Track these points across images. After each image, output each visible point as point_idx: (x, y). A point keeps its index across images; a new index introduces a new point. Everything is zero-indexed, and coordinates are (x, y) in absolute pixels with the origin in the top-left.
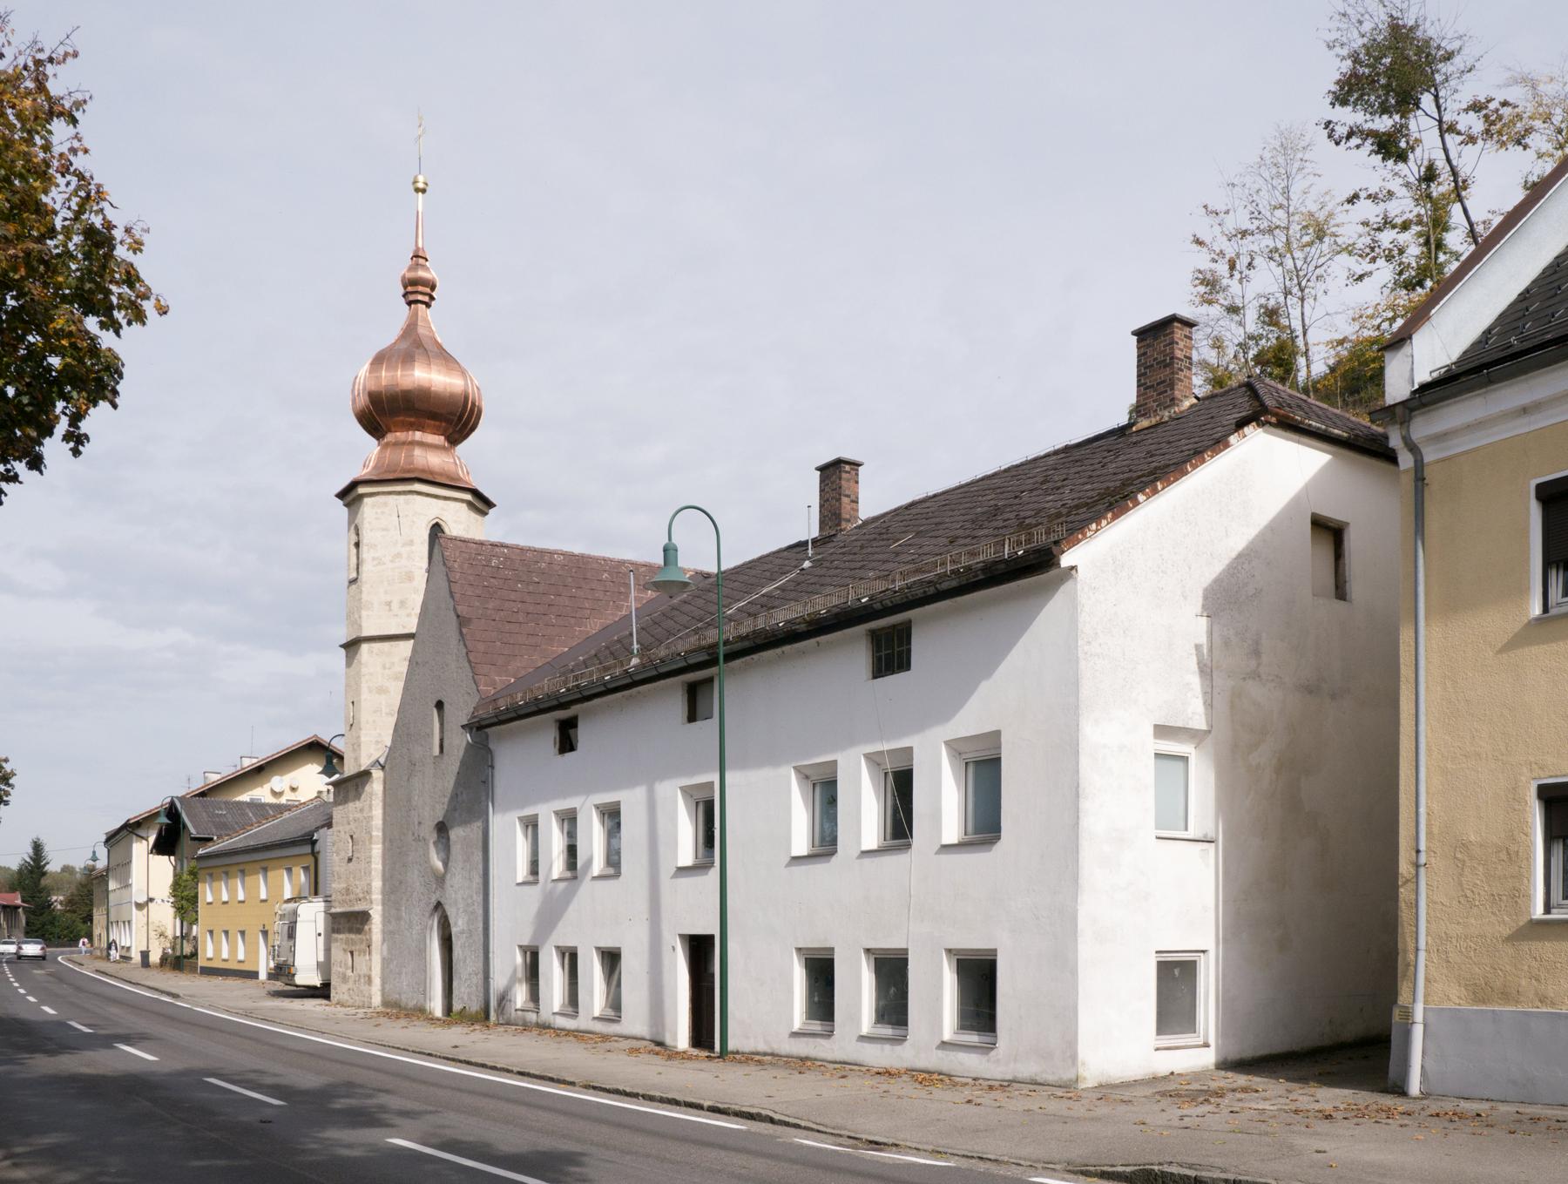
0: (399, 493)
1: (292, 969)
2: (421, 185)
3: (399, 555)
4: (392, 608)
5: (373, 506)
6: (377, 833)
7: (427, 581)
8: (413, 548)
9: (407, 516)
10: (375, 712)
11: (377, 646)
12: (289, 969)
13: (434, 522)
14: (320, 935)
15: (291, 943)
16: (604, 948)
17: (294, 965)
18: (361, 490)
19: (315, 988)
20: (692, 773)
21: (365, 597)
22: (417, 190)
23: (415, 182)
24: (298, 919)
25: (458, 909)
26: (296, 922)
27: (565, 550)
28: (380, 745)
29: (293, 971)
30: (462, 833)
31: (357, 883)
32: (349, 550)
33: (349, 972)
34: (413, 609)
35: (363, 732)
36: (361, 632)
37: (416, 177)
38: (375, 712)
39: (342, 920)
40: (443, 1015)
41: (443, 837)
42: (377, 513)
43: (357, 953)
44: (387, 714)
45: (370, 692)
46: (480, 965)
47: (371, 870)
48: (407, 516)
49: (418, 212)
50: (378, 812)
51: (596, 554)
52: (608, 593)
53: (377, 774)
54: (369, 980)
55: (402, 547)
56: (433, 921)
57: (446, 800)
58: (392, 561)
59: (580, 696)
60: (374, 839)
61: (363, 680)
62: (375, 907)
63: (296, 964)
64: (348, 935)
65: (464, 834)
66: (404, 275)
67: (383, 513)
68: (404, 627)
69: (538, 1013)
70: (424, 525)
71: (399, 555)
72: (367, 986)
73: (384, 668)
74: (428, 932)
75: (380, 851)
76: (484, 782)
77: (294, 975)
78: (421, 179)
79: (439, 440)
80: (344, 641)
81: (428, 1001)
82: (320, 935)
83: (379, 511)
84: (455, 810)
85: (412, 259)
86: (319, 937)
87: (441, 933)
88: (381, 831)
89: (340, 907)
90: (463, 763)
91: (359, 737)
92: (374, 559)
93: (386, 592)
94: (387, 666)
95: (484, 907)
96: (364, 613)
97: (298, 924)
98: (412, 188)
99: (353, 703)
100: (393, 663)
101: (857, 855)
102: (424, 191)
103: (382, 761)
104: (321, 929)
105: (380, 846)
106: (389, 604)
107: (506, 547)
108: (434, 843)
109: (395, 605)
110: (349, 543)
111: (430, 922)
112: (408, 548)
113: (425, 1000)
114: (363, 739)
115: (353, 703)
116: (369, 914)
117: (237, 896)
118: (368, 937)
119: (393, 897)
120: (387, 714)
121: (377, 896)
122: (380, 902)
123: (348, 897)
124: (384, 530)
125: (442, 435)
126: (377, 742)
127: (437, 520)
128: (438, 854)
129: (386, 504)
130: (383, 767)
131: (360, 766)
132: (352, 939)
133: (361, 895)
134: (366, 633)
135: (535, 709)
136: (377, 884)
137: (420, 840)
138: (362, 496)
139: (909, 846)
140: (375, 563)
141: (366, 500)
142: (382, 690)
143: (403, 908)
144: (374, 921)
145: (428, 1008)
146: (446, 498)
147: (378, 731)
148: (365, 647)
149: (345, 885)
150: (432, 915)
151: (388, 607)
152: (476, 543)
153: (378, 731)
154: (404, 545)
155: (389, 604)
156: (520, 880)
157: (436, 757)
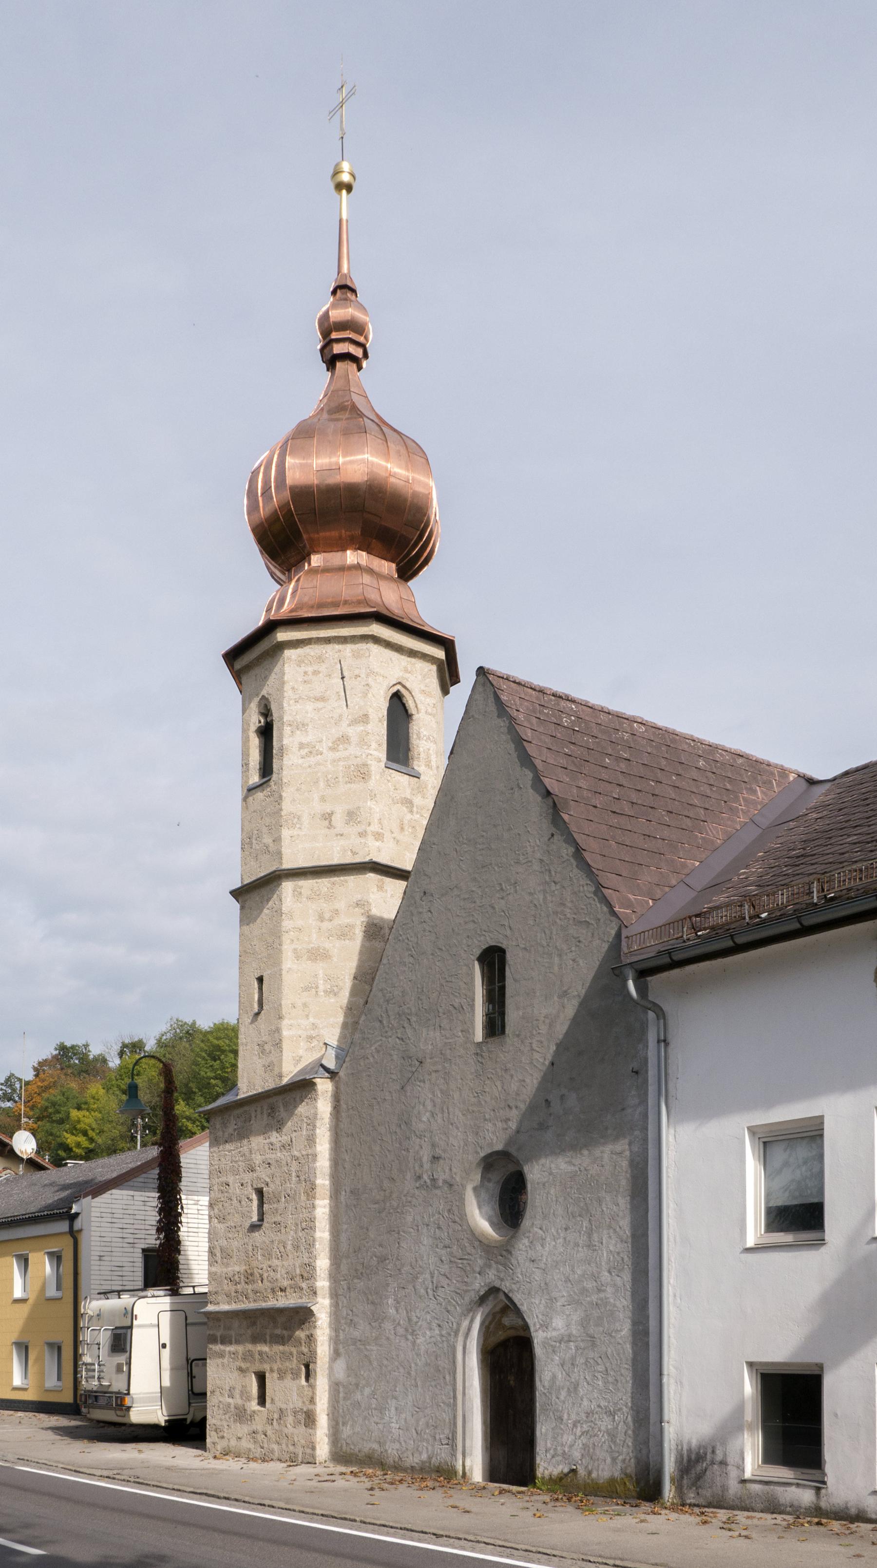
0: (344, 640)
1: (127, 1399)
2: (345, 178)
3: (344, 739)
4: (333, 823)
5: (300, 663)
6: (323, 1182)
7: (451, 753)
8: (369, 727)
9: (357, 676)
10: (307, 989)
11: (307, 884)
12: (123, 1399)
13: (395, 689)
14: (164, 1346)
15: (121, 1359)
16: (761, 1364)
17: (128, 1394)
18: (282, 636)
19: (156, 1426)
20: (769, 1103)
21: (287, 806)
22: (340, 186)
23: (337, 172)
24: (135, 1322)
25: (553, 1300)
26: (131, 1327)
27: (646, 718)
28: (315, 1043)
29: (128, 1401)
30: (563, 1166)
31: (275, 1262)
32: (246, 741)
33: (254, 1405)
34: (369, 824)
35: (285, 1023)
36: (281, 864)
37: (338, 165)
38: (307, 989)
39: (236, 1323)
40: (484, 1479)
41: (489, 1180)
42: (306, 673)
43: (275, 1375)
44: (325, 991)
45: (298, 958)
46: (624, 1396)
47: (314, 1241)
48: (357, 676)
49: (341, 221)
50: (323, 1147)
51: (682, 731)
52: (714, 789)
53: (324, 1086)
54: (310, 1419)
55: (349, 725)
56: (472, 1321)
57: (515, 1114)
58: (333, 749)
59: (798, 926)
60: (318, 1190)
61: (286, 939)
62: (319, 1299)
63: (132, 1392)
64: (249, 1346)
65: (571, 1168)
66: (326, 315)
67: (316, 673)
68: (354, 853)
69: (818, 1489)
70: (382, 692)
71: (344, 739)
72: (302, 1429)
73: (321, 918)
74: (461, 1339)
75: (327, 1210)
76: (637, 1073)
77: (129, 1408)
78: (346, 166)
79: (388, 567)
80: (238, 884)
81: (460, 1457)
82: (164, 1346)
83: (310, 669)
84: (542, 1126)
85: (334, 292)
86: (163, 1350)
87: (482, 1342)
88: (327, 1177)
89: (229, 1303)
90: (562, 1047)
91: (278, 1030)
92: (301, 746)
93: (323, 799)
94: (327, 916)
95: (634, 1294)
96: (285, 833)
97: (134, 1331)
98: (332, 186)
99: (260, 980)
100: (336, 912)
101: (740, 1251)
102: (349, 188)
103: (331, 1064)
104: (166, 1338)
105: (327, 1202)
106: (328, 817)
107: (573, 701)
108: (475, 1189)
109: (338, 819)
110: (245, 731)
111: (465, 1323)
112: (360, 728)
113: (453, 1455)
114: (285, 1033)
115: (260, 980)
116: (311, 1311)
117: (12, 1292)
118: (305, 1350)
119: (360, 1284)
120: (325, 991)
121: (323, 1283)
122: (327, 1291)
123: (250, 1287)
124: (317, 699)
125: (392, 561)
126: (310, 1038)
127: (398, 687)
128: (480, 1207)
129: (320, 659)
130: (332, 1074)
131: (280, 1076)
132: (260, 1353)
133: (285, 1283)
134: (287, 864)
135: (796, 926)
136: (323, 1264)
137: (436, 1187)
138: (281, 646)
139: (821, 1242)
140: (304, 752)
141: (288, 653)
142: (317, 955)
143: (390, 1301)
144: (319, 1323)
145: (460, 1468)
146: (412, 653)
147: (311, 1020)
148: (287, 887)
149: (242, 1268)
150: (470, 1310)
151: (326, 823)
152: (534, 690)
153: (311, 1020)
154: (354, 722)
155: (328, 817)
156: (750, 1243)
157: (478, 1044)
